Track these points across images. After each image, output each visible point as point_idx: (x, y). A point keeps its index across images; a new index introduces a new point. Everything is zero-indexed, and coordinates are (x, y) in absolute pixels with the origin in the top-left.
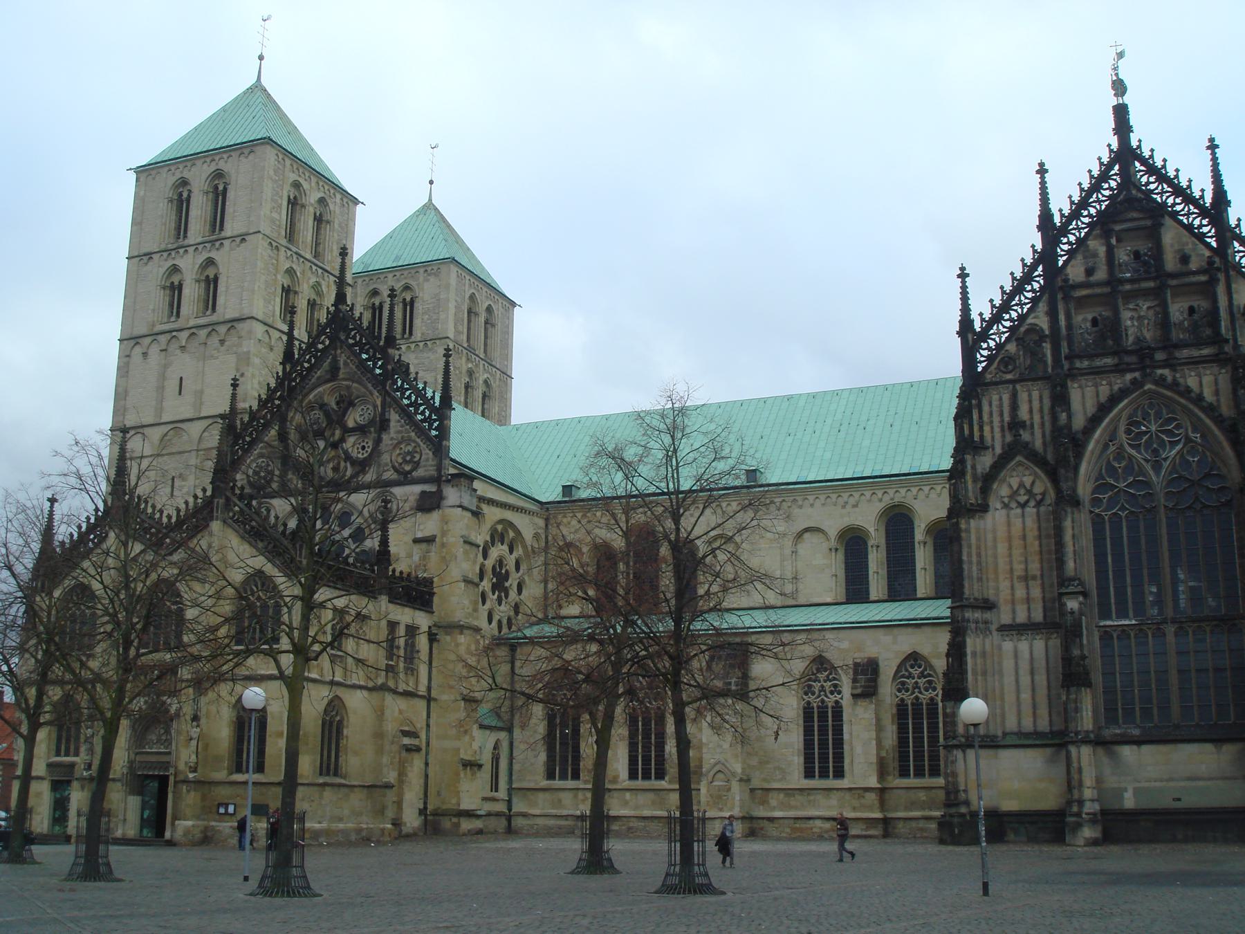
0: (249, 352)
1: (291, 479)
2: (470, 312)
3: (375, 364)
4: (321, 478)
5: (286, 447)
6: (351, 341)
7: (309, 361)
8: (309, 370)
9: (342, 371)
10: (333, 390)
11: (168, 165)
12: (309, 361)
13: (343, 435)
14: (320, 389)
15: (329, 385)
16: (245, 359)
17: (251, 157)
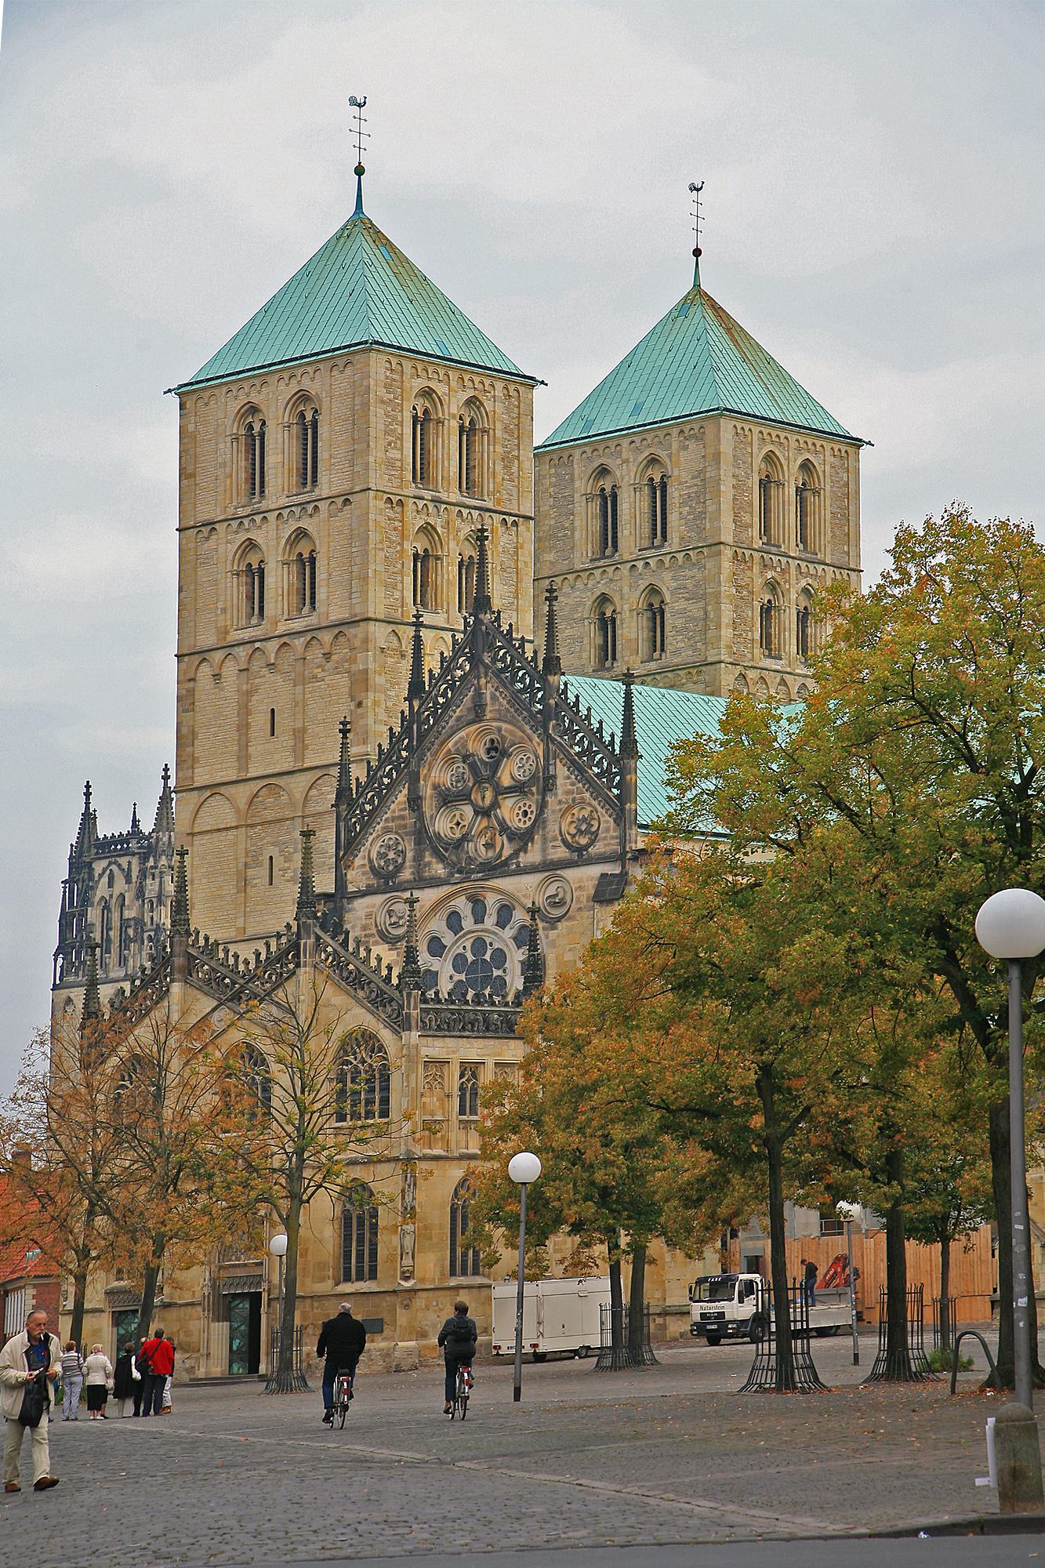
0: (366, 671)
1: (430, 863)
2: (765, 484)
3: (533, 696)
4: (470, 860)
5: (421, 817)
6: (500, 665)
7: (444, 695)
8: (446, 706)
9: (489, 708)
10: (480, 733)
11: (226, 383)
12: (444, 695)
13: (496, 798)
14: (462, 733)
15: (473, 728)
16: (360, 682)
17: (349, 371)
